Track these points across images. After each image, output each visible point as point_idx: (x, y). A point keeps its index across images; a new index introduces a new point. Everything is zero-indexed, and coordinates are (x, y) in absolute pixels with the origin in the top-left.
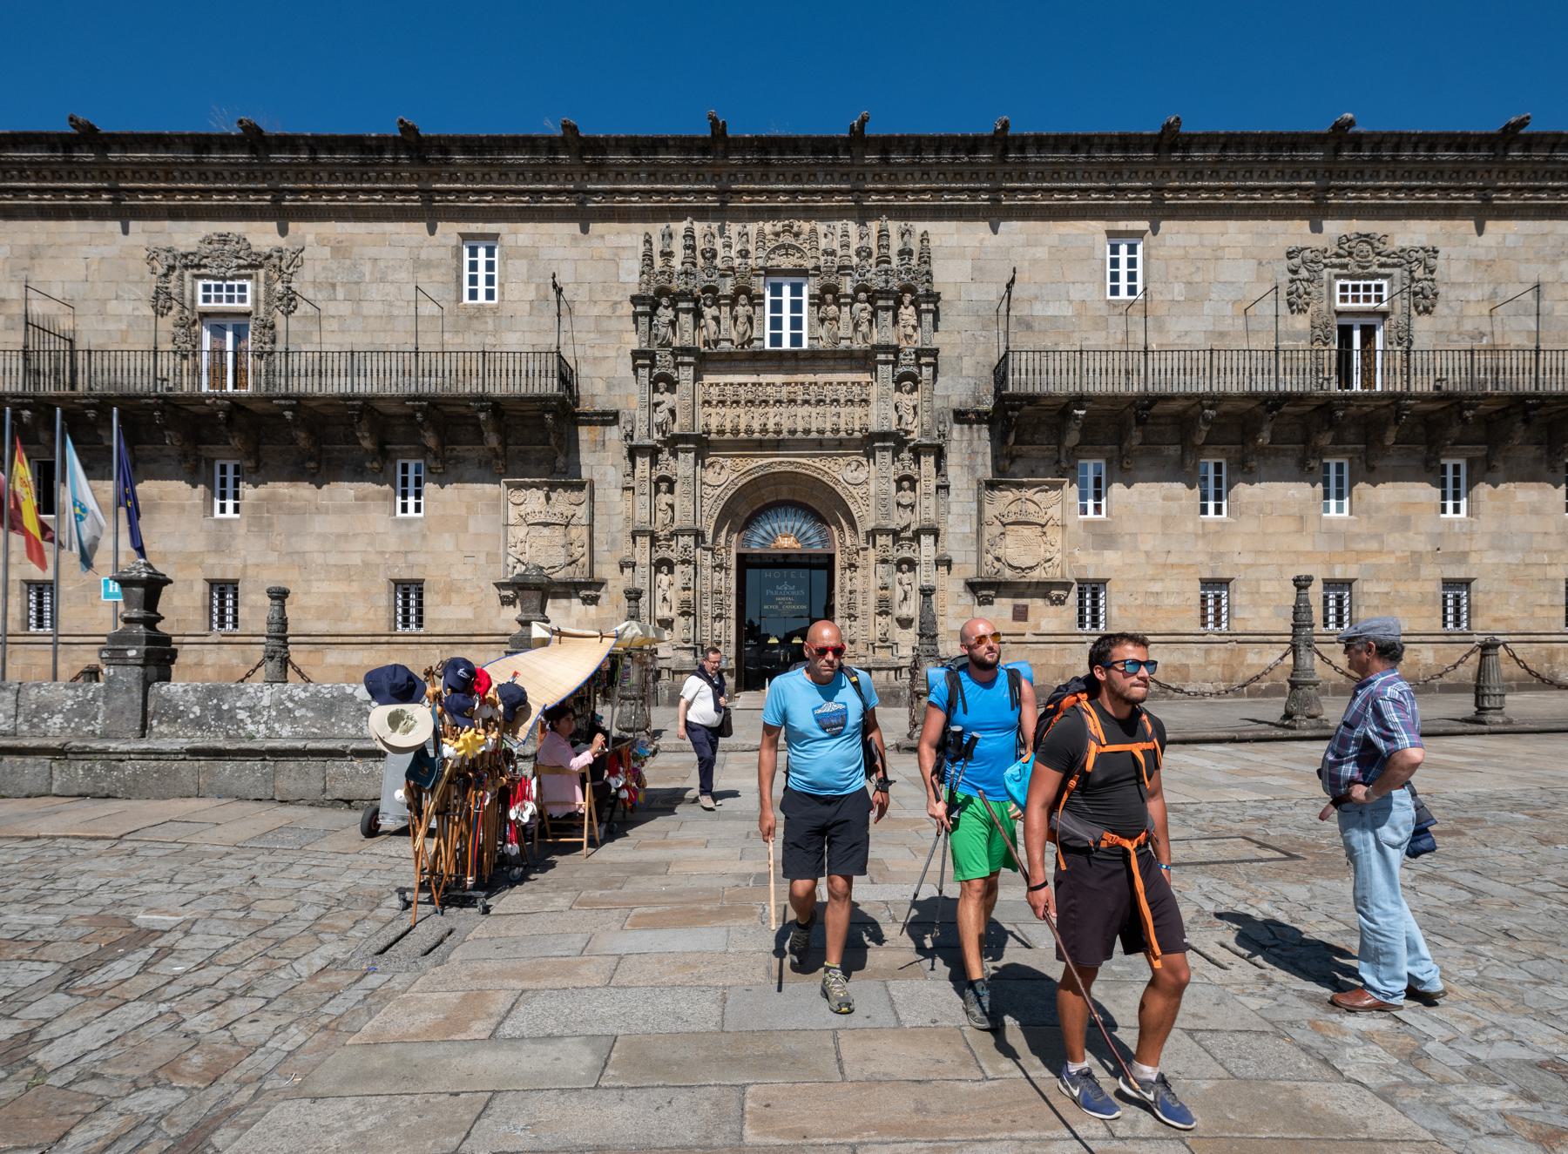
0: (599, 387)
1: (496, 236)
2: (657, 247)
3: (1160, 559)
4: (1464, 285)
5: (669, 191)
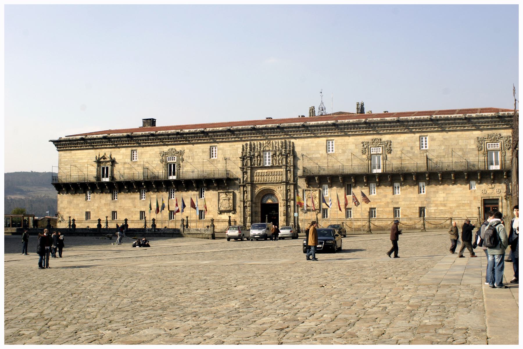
0: (235, 173)
2: (245, 146)
4: (397, 148)
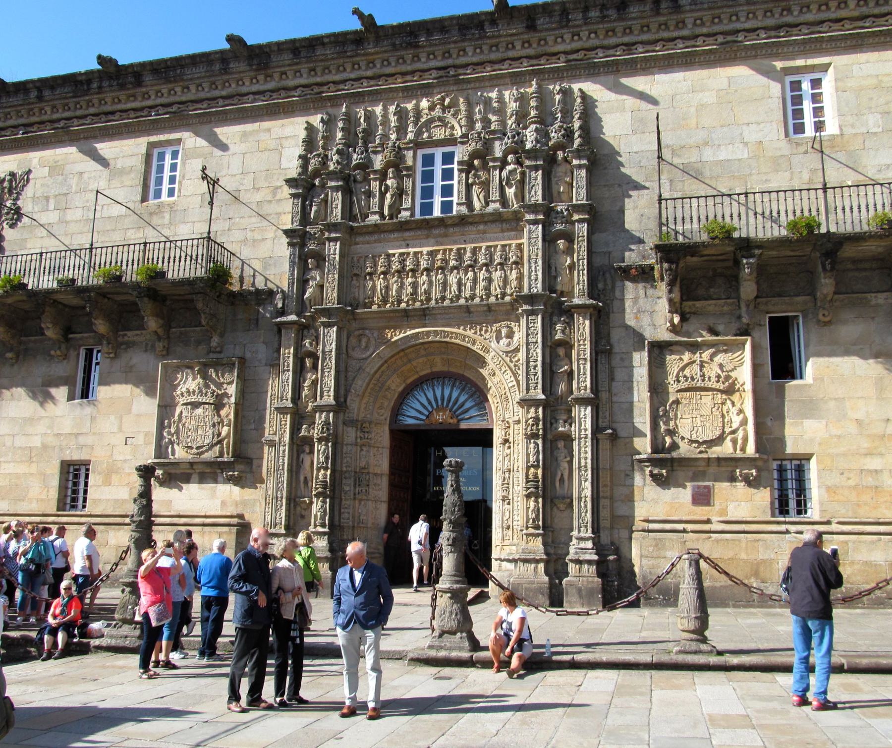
1: (179, 141)
3: (878, 429)
5: (328, 83)
